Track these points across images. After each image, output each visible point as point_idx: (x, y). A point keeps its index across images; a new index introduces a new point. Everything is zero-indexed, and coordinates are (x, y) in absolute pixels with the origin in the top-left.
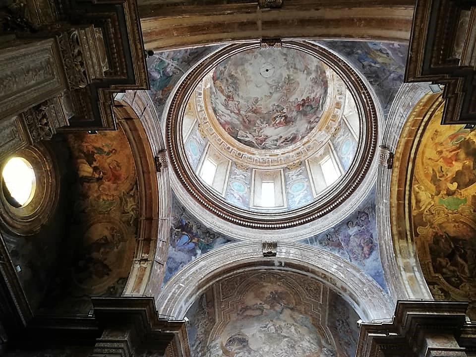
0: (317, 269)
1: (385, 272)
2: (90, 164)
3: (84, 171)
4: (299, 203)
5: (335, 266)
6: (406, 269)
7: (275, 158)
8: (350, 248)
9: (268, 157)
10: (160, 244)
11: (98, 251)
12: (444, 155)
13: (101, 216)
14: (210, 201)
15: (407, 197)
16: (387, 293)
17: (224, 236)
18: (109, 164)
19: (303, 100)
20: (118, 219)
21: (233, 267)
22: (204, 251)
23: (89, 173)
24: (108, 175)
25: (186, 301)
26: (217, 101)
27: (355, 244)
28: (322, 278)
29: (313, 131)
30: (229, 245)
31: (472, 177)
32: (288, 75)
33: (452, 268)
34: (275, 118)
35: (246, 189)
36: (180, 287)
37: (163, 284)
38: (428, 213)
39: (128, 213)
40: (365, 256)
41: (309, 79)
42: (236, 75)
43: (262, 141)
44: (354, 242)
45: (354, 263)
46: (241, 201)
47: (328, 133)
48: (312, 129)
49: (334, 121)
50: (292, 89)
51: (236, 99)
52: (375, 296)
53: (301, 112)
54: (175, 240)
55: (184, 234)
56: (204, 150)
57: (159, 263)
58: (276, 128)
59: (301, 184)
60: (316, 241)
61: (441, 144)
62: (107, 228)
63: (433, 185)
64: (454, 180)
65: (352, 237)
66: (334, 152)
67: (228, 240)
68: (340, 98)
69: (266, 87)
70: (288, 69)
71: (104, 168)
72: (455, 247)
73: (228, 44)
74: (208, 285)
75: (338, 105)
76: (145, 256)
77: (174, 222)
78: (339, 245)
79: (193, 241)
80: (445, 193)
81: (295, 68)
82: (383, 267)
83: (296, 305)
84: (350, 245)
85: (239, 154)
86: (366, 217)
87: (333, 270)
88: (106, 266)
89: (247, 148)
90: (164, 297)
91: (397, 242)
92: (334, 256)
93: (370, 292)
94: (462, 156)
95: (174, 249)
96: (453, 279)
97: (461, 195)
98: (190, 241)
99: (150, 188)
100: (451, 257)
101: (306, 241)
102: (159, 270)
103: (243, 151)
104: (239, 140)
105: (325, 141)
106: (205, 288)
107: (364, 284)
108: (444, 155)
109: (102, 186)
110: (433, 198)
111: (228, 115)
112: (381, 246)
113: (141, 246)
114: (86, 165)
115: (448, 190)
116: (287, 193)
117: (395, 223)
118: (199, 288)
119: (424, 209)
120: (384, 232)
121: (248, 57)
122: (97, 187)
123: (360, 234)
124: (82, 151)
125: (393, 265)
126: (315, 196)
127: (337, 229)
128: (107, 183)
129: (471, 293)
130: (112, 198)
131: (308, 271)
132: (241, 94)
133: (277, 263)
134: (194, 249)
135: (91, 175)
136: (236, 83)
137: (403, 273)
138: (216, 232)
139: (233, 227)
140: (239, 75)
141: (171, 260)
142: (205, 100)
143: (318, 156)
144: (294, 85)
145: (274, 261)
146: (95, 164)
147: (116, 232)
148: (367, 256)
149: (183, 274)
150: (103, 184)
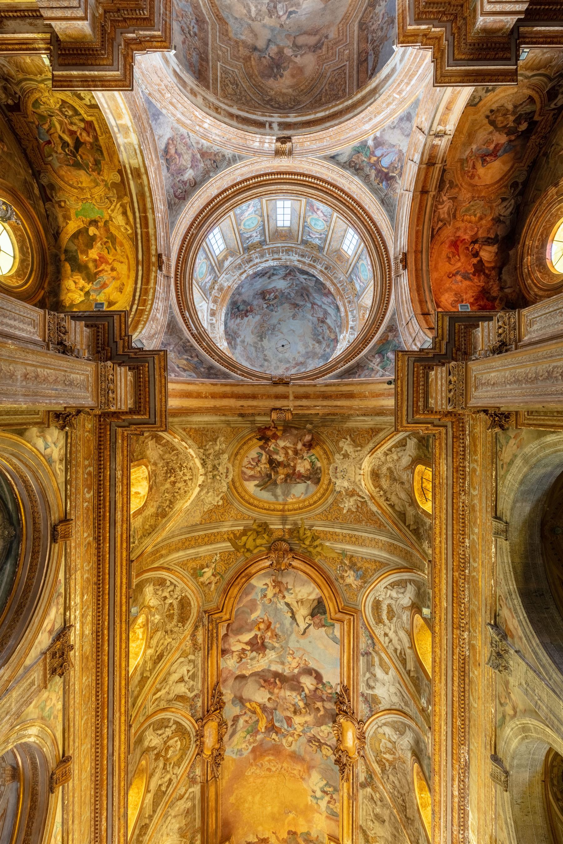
0: (227, 120)
1: (148, 122)
2: (481, 261)
3: (490, 252)
4: (249, 205)
5: (206, 126)
6: (124, 129)
7: (276, 256)
8: (190, 152)
9: (284, 257)
10: (417, 157)
11: (497, 145)
12: (109, 267)
13: (483, 194)
14: (352, 210)
15: (138, 220)
16: (142, 91)
17: (338, 164)
18: (459, 260)
19: (247, 316)
20: (463, 190)
21: (329, 121)
22: (364, 145)
23: (484, 250)
24: (463, 247)
25: (393, 70)
26: (334, 318)
27: (185, 157)
28: (221, 108)
29: (236, 286)
30: (332, 152)
31: (76, 241)
32: (262, 341)
33: (74, 128)
34: (275, 298)
35: (309, 220)
36: (400, 93)
37: (421, 97)
38: (112, 199)
39: (449, 199)
40: (173, 141)
41: (242, 337)
42: (314, 342)
43: (289, 274)
44: (185, 160)
45: (183, 131)
46: (315, 208)
47: (221, 284)
48: (237, 288)
49: (216, 296)
50: (258, 327)
51: (315, 320)
52: (157, 87)
53: (249, 304)
54: (399, 161)
55: (385, 168)
56: (353, 269)
57: (421, 129)
58: (275, 287)
59: (247, 227)
60: (229, 160)
61: (114, 278)
62: (479, 178)
63: (113, 232)
64: (93, 239)
65: (189, 166)
66: (214, 264)
67: (333, 158)
68: (212, 320)
69: (285, 330)
70: (263, 347)
71: (467, 256)
72: (75, 157)
73: (320, 381)
74: (364, 93)
75: (213, 314)
76: (437, 141)
77: (396, 185)
78: (203, 154)
79: (375, 159)
80: (99, 224)
81: (256, 347)
82: (151, 129)
83: (250, 58)
84: (190, 155)
85: (314, 261)
86: (177, 194)
87: (208, 121)
88: (492, 123)
89: (306, 268)
90: (421, 79)
91: (141, 165)
92: (207, 139)
93: (163, 92)
94: (91, 265)
95: (401, 148)
96: (70, 113)
97: (83, 221)
98: (379, 158)
99: (417, 232)
100: (78, 144)
101: (241, 158)
102: (423, 119)
103: (310, 265)
104: (314, 276)
105: (223, 275)
106: (368, 89)
107: (171, 103)
108: (109, 267)
109: (473, 233)
110: (110, 217)
111: (324, 304)
112: (157, 157)
113: (441, 154)
114: (486, 259)
115: (97, 227)
116: (262, 216)
117: (146, 189)
118: (374, 91)
119: (117, 203)
120: (156, 176)
121: (301, 359)
122: (480, 232)
123: (181, 171)
124: (487, 276)
125: (141, 133)
126: (231, 213)
127: (206, 176)
128: (467, 237)
129: (47, 94)
130: (465, 218)
131: (237, 117)
132: (310, 324)
133: (275, 126)
135: (484, 247)
136: (315, 335)
137: (129, 124)
138: (347, 169)
139: (327, 175)
140: (311, 342)
141: (406, 133)
142: (348, 322)
143: (230, 259)
144: (256, 331)
145: (279, 130)
146: (475, 261)
147: (469, 172)
148: (171, 142)
149: (394, 111)
150: (472, 237)
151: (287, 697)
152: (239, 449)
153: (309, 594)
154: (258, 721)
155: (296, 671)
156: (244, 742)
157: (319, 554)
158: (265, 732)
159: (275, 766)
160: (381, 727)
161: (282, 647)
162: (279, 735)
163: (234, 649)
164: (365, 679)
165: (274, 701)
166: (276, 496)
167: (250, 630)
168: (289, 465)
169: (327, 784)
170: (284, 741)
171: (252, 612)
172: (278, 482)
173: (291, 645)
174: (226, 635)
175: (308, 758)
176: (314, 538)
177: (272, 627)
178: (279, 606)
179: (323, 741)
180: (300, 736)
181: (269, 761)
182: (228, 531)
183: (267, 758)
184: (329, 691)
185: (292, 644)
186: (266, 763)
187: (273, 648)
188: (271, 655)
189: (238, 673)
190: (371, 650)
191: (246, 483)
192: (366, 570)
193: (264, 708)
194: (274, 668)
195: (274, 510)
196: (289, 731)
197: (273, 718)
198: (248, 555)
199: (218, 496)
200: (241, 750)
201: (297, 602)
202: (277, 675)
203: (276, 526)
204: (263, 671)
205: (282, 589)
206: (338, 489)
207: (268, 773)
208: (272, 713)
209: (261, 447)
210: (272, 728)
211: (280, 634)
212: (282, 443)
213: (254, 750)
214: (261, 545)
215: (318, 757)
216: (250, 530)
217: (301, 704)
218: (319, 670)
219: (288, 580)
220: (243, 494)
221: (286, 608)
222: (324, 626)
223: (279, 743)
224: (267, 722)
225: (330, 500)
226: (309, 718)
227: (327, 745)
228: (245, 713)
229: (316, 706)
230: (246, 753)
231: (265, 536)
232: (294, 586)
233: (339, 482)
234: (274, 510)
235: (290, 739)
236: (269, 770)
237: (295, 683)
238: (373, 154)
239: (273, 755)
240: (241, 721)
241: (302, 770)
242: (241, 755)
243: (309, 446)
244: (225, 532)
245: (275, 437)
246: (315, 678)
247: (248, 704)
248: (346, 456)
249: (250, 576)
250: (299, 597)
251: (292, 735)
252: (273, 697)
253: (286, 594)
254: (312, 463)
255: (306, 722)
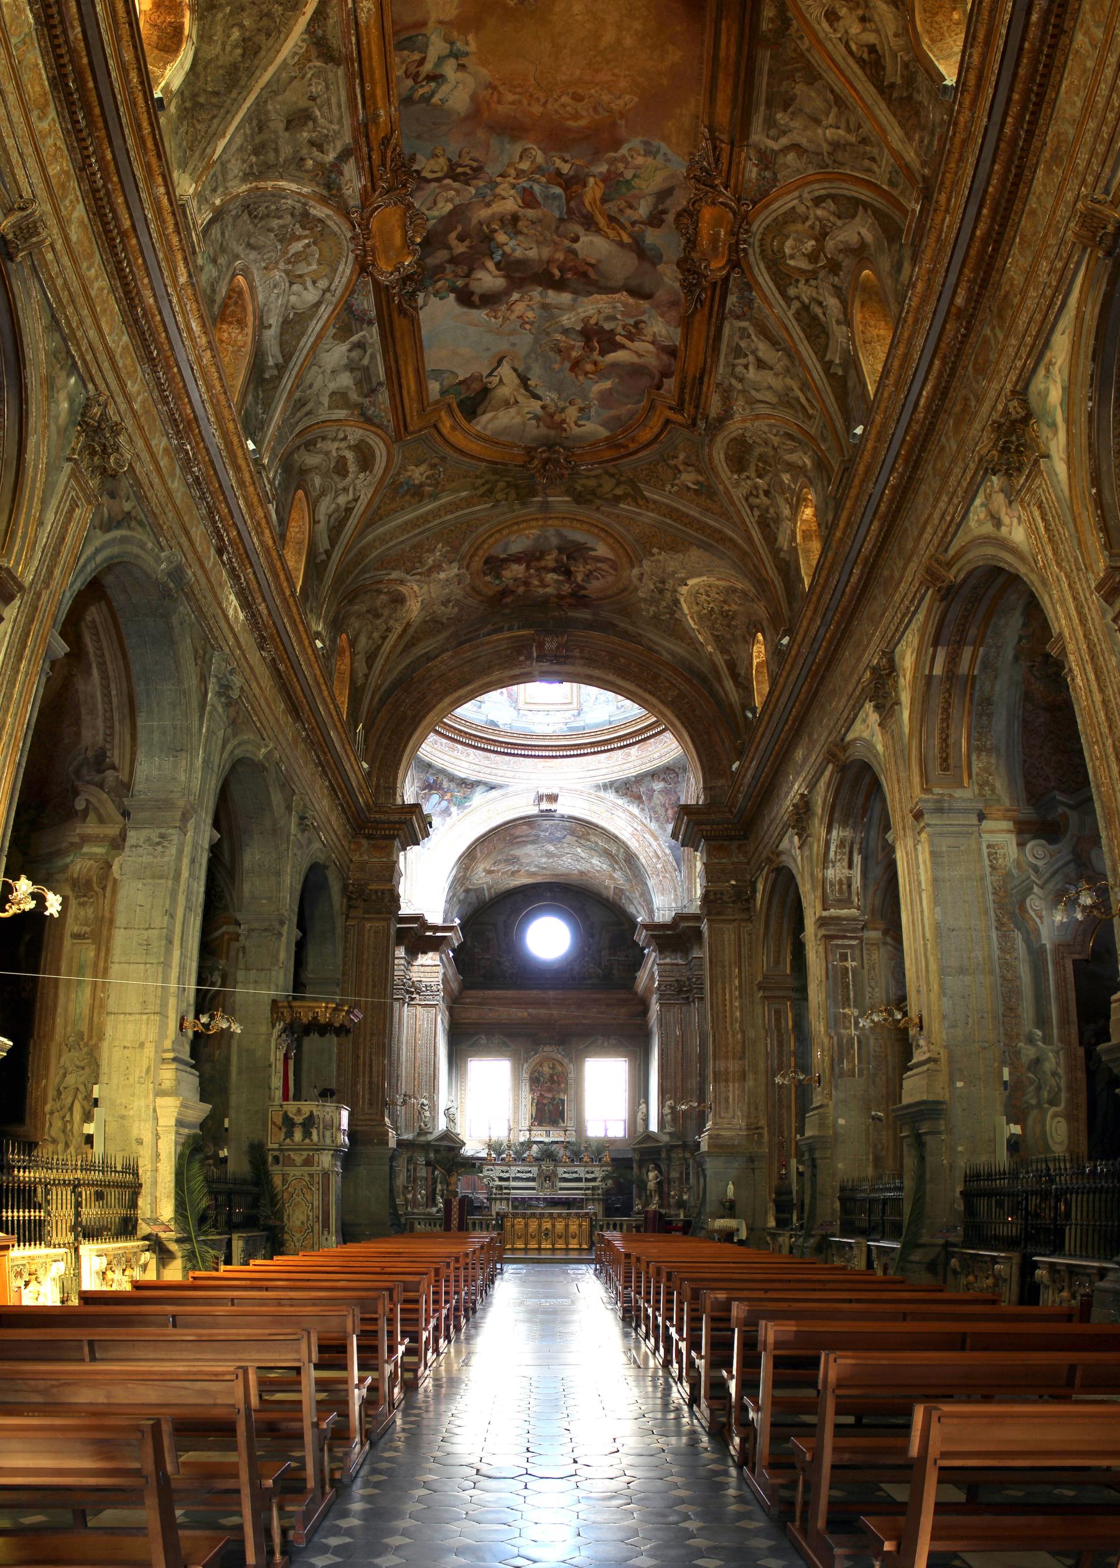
17: (485, 784)
30: (494, 793)
45: (653, 826)
101: (598, 787)
123: (665, 792)
127: (640, 779)
134: (448, 808)
151: (534, 245)
152: (618, 594)
153: (494, 418)
154: (604, 200)
155: (516, 296)
156: (637, 167)
157: (477, 477)
158: (588, 175)
159: (564, 106)
160: (324, 292)
161: (548, 334)
162: (552, 169)
163: (650, 347)
164: (369, 351)
165: (564, 236)
166: (559, 534)
167: (614, 365)
168: (537, 570)
169: (426, 99)
170: (540, 158)
171: (610, 391)
172: (555, 554)
173: (529, 338)
174: (666, 374)
175: (481, 134)
176: (491, 491)
177: (567, 365)
178: (555, 396)
179: (448, 181)
180: (501, 175)
181: (576, 116)
182: (647, 509)
183: (582, 123)
184: (440, 284)
185: (525, 340)
186: (584, 113)
187: (566, 331)
188: (568, 320)
189: (645, 304)
190: (366, 402)
191: (610, 555)
192: (393, 499)
193: (589, 223)
194: (566, 297)
195: (564, 518)
196: (530, 179)
197: (568, 202)
198: (612, 470)
199: (658, 561)
200: (647, 153)
201: (517, 402)
202: (560, 286)
203: (560, 500)
204: (590, 294)
205: (548, 419)
206: (455, 565)
207: (580, 91)
208: (570, 211)
209: (585, 588)
210: (571, 183)
211: (552, 354)
212: (549, 590)
213: (617, 144)
214: (588, 477)
215: (454, 146)
216: (607, 500)
217: (501, 237)
218: (466, 310)
219: (534, 430)
220: (616, 546)
221: (540, 393)
222: (461, 383)
223: (552, 153)
224: (580, 197)
225: (465, 548)
226: (484, 213)
227: (437, 180)
228: (633, 223)
229: (467, 243)
230: (636, 142)
231: (579, 488)
232: (524, 424)
233: (456, 571)
234: (564, 518)
235: (525, 166)
236: (578, 98)
237: (517, 275)
238: (449, 801)
239: (568, 130)
240: (643, 210)
241: (493, 105)
242: (646, 143)
243: (504, 593)
244: (652, 511)
245: (560, 597)
246: (472, 293)
247: (626, 239)
248: (445, 604)
249: (611, 443)
250: (513, 411)
251: (520, 174)
252: (567, 243)
253: (540, 412)
254: (498, 576)
255: (488, 205)
